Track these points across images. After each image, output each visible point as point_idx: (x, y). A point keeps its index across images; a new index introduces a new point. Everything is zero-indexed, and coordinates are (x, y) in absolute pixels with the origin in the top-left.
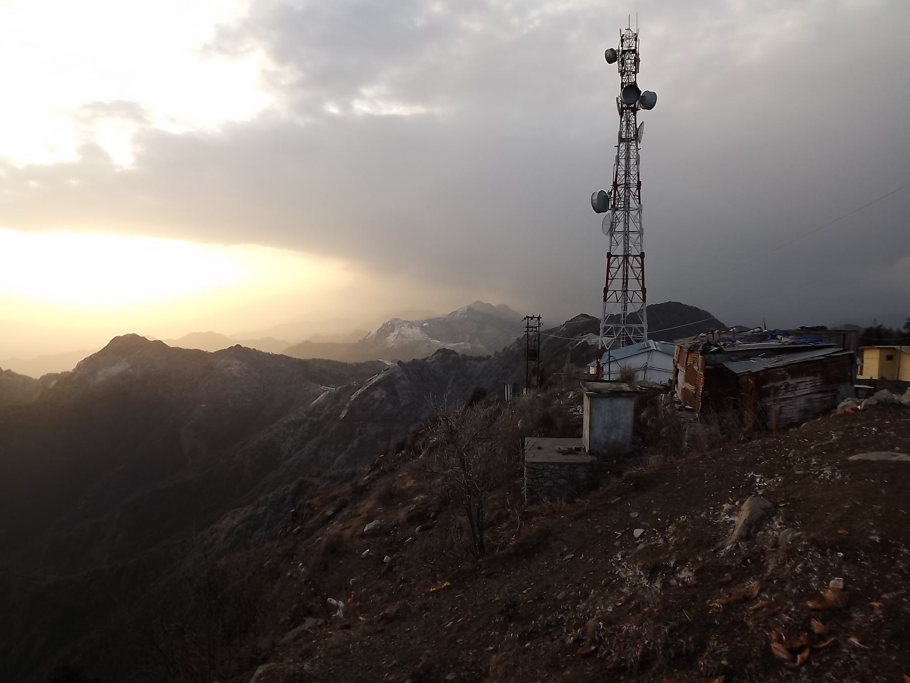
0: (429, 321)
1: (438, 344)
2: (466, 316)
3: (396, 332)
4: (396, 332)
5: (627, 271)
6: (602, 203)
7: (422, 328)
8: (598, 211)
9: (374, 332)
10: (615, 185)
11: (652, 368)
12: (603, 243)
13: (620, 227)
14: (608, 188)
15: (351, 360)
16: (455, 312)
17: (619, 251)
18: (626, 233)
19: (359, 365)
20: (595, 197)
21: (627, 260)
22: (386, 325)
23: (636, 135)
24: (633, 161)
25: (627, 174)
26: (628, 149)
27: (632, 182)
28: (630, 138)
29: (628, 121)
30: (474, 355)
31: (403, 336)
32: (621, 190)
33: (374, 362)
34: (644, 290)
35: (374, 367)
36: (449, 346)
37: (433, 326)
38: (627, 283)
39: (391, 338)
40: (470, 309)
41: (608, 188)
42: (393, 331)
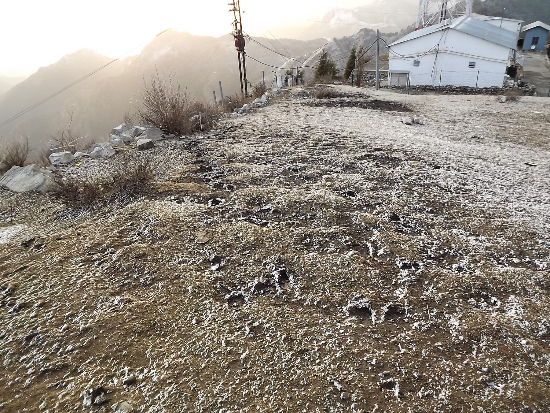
1: (365, 25)
3: (336, 17)
4: (336, 17)
15: (305, 39)
19: (310, 42)
33: (319, 40)
39: (333, 21)
42: (333, 16)
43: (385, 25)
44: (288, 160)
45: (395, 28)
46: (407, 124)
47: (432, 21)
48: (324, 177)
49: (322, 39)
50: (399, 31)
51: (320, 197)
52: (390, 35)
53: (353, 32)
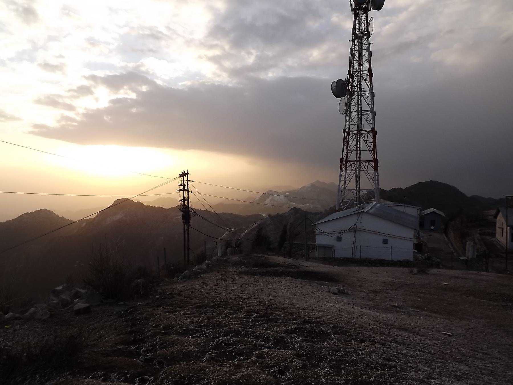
0: (289, 192)
1: (294, 205)
2: (310, 189)
3: (270, 198)
4: (270, 198)
5: (360, 144)
6: (341, 89)
7: (286, 196)
8: (338, 96)
9: (257, 198)
10: (351, 74)
11: (362, 230)
12: (340, 121)
13: (354, 108)
14: (345, 77)
15: (243, 214)
16: (304, 187)
17: (354, 128)
18: (359, 113)
19: (248, 217)
20: (334, 85)
21: (359, 137)
22: (265, 194)
23: (367, 29)
24: (364, 52)
25: (360, 65)
26: (360, 45)
27: (364, 69)
28: (361, 35)
29: (361, 19)
30: (313, 212)
31: (274, 201)
32: (356, 79)
34: (376, 161)
35: (257, 217)
36: (300, 206)
37: (290, 195)
38: (360, 154)
39: (267, 201)
40: (313, 185)
41: (345, 77)
42: (268, 197)
43: (311, 206)
44: (221, 333)
45: (320, 208)
46: (334, 293)
47: (349, 204)
48: (256, 352)
49: (259, 215)
50: (323, 210)
51: (250, 376)
52: (316, 214)
53: (285, 210)
